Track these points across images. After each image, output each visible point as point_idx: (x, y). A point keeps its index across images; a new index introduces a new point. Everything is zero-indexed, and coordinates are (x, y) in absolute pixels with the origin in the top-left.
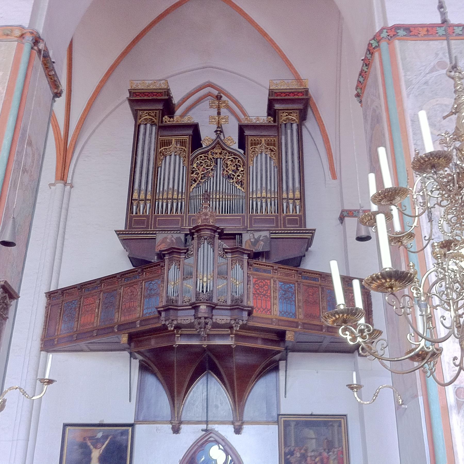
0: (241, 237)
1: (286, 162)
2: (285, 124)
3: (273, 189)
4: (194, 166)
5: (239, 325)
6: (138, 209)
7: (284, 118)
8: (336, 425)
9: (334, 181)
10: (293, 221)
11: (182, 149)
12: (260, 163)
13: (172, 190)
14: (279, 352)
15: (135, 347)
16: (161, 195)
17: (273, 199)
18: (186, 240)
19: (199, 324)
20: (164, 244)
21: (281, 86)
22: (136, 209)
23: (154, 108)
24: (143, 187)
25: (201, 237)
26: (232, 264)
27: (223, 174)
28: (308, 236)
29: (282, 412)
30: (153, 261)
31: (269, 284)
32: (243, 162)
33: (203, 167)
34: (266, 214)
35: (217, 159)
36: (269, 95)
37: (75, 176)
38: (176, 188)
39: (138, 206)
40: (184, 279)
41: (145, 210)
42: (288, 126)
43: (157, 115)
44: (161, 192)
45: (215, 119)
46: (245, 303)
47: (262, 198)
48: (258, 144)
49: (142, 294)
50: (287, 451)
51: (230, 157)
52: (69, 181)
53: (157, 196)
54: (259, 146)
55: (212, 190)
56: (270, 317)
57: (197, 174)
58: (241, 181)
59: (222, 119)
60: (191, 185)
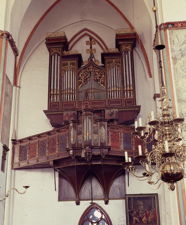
1: (126, 71)
2: (124, 52)
3: (119, 86)
5: (104, 155)
7: (124, 48)
8: (153, 198)
9: (150, 79)
10: (129, 102)
11: (73, 67)
12: (113, 74)
17: (119, 91)
20: (67, 117)
23: (58, 46)
24: (55, 88)
26: (100, 127)
27: (94, 79)
28: (137, 109)
29: (127, 194)
30: (62, 125)
33: (84, 76)
35: (91, 71)
38: (71, 87)
39: (53, 97)
42: (126, 52)
43: (60, 50)
44: (64, 90)
45: (89, 51)
46: (107, 145)
47: (114, 91)
48: (111, 63)
50: (130, 211)
51: (97, 70)
52: (18, 85)
53: (62, 92)
55: (89, 88)
56: (119, 150)
59: (93, 50)
60: (79, 86)
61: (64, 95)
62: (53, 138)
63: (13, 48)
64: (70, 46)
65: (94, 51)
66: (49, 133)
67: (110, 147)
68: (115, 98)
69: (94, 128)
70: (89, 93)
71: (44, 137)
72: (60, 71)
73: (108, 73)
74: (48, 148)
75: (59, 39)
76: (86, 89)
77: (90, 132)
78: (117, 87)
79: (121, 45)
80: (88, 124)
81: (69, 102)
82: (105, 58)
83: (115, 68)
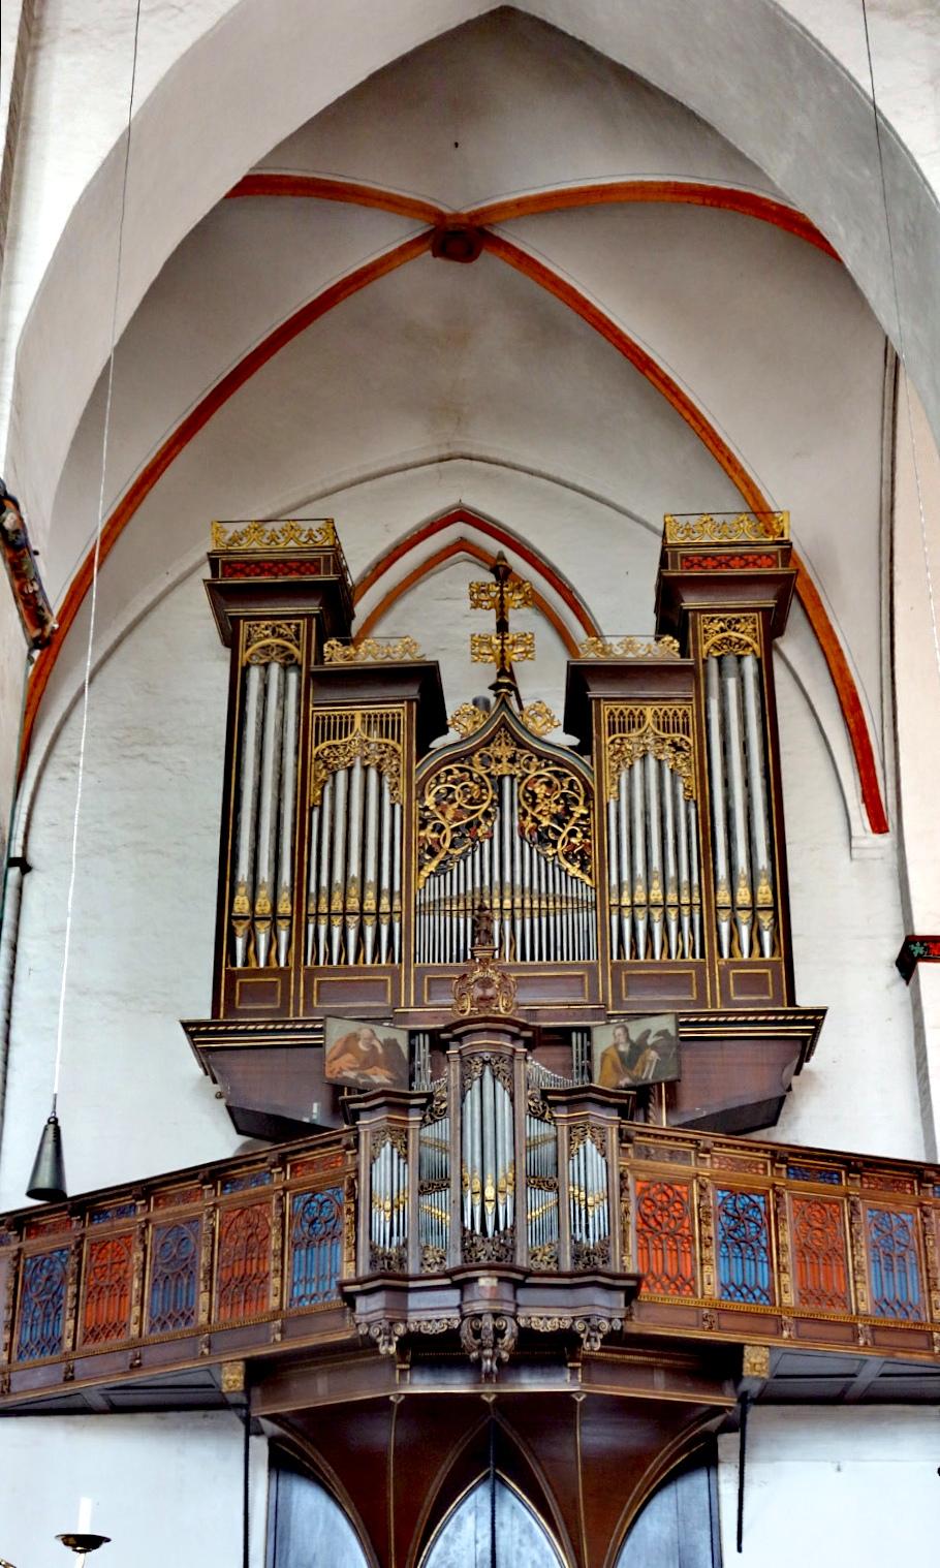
0: (589, 1039)
1: (727, 783)
4: (427, 803)
5: (600, 1336)
6: (252, 948)
9: (878, 837)
11: (387, 745)
13: (358, 885)
14: (716, 1411)
15: (264, 1402)
16: (323, 900)
17: (685, 910)
18: (412, 1049)
19: (477, 1334)
21: (703, 533)
22: (247, 949)
24: (265, 874)
25: (473, 1055)
27: (522, 829)
28: (799, 1031)
30: (306, 1120)
31: (684, 1196)
32: (588, 789)
33: (455, 806)
34: (665, 958)
35: (502, 777)
36: (663, 563)
37: (33, 832)
38: (371, 876)
39: (251, 937)
40: (422, 1191)
41: (273, 953)
42: (730, 662)
45: (490, 644)
47: (649, 905)
48: (632, 725)
49: (283, 1235)
51: (542, 772)
53: (312, 905)
54: (635, 733)
55: (487, 883)
56: (692, 1301)
57: (439, 829)
58: (582, 852)
59: (514, 643)
60: (421, 868)
61: (323, 921)
62: (243, 1210)
63: (22, 593)
64: (363, 608)
65: (522, 649)
66: (216, 1174)
67: (638, 1278)
68: (657, 957)
69: (532, 1145)
70: (497, 915)
71: (187, 1197)
72: (296, 765)
73: (609, 789)
74: (211, 1279)
75: (294, 565)
76: (469, 888)
77: (505, 1176)
78: (668, 882)
79: (695, 619)
80: (490, 1120)
81: (350, 969)
82: (591, 695)
83: (660, 762)
